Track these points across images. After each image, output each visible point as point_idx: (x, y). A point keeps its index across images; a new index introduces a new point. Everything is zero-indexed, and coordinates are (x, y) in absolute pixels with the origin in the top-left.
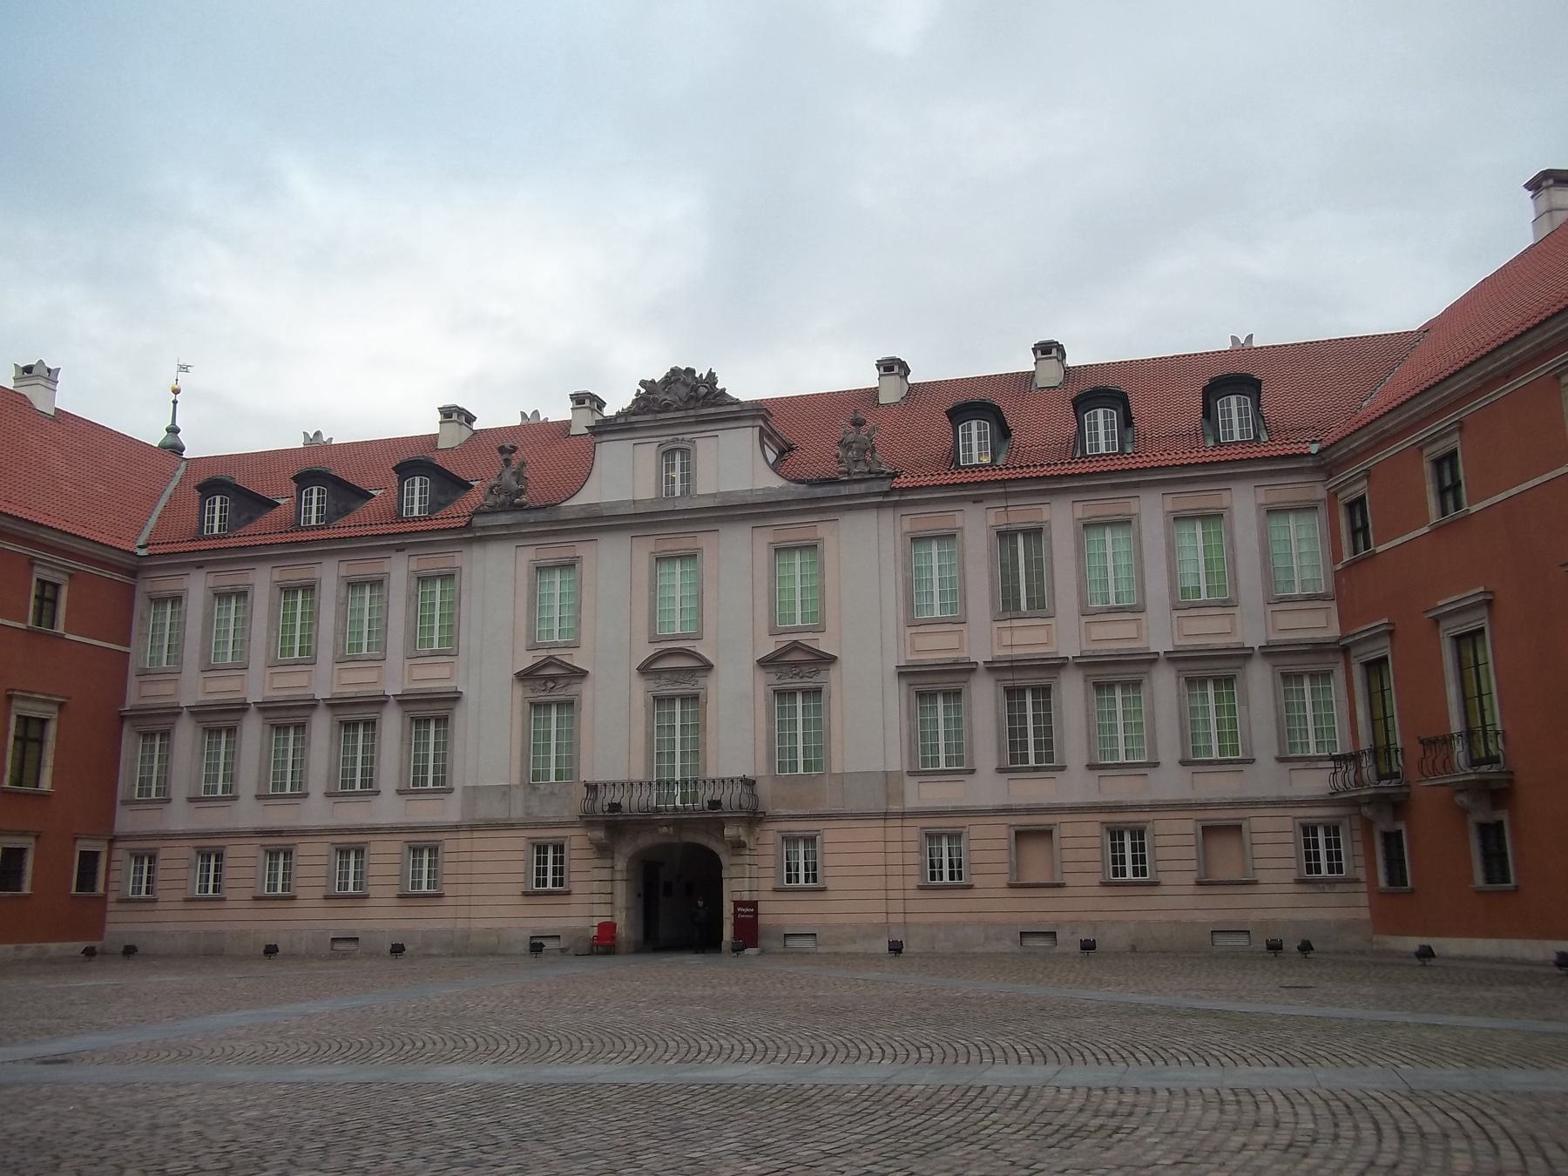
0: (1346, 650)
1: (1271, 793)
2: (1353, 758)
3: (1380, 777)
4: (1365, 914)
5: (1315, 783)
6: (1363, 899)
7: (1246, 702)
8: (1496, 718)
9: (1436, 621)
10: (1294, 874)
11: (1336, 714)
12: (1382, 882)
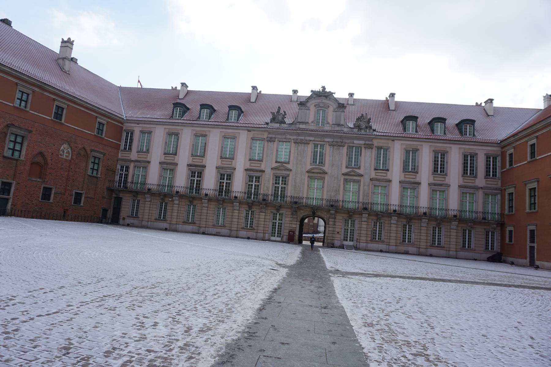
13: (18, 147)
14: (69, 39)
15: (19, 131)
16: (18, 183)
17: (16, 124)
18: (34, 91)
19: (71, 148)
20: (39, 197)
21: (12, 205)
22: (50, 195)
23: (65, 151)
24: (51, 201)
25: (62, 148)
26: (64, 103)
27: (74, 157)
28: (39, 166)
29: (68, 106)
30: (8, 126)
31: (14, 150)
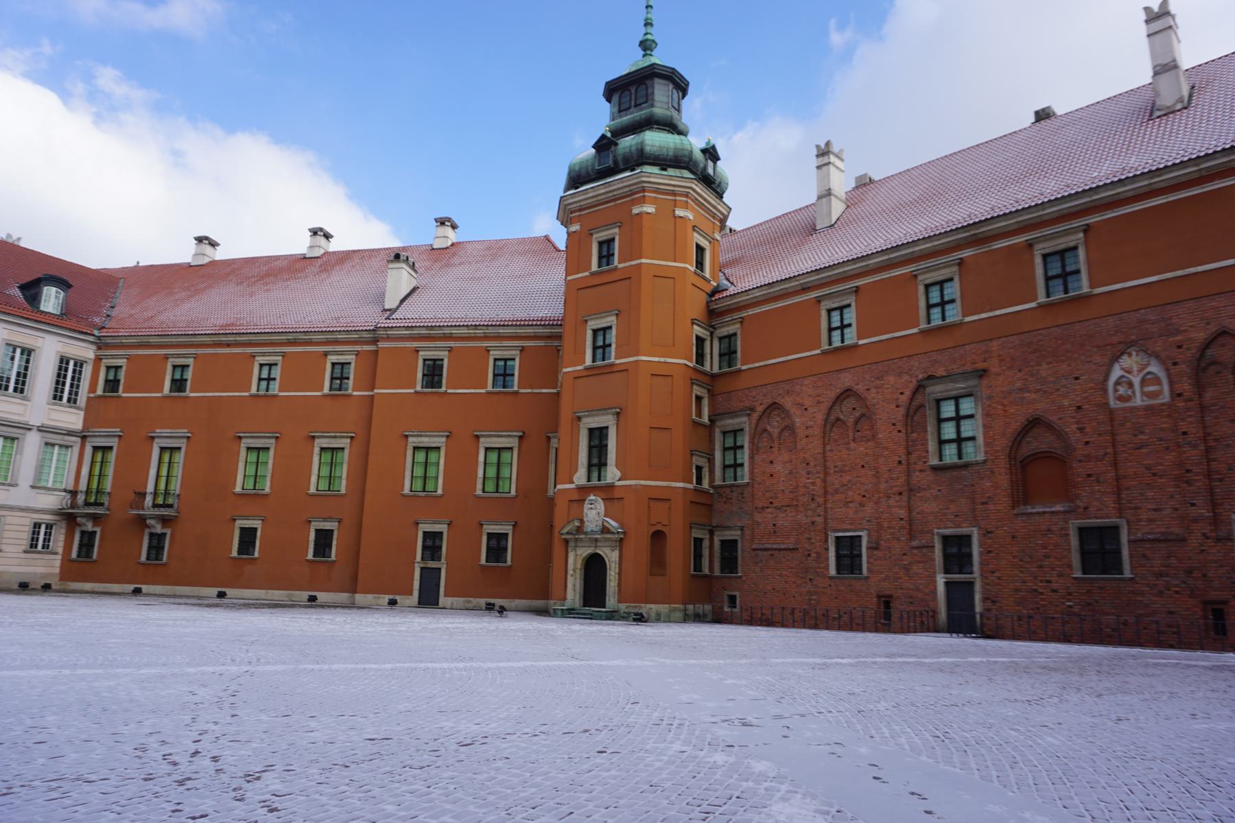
0: (84, 438)
1: (23, 504)
2: (74, 493)
3: (87, 504)
4: (57, 571)
5: (51, 501)
6: (58, 563)
7: (20, 451)
8: (176, 486)
9: (153, 438)
10: (24, 548)
11: (65, 469)
12: (74, 555)
13: (967, 429)
14: (1147, 9)
15: (951, 386)
16: (986, 533)
17: (940, 372)
18: (961, 263)
19: (1158, 357)
20: (1070, 566)
21: (985, 599)
22: (1118, 552)
23: (1136, 379)
24: (1127, 574)
25: (1117, 372)
26: (1066, 233)
27: (1186, 386)
28: (1036, 463)
29: (1087, 229)
30: (920, 388)
31: (959, 440)
